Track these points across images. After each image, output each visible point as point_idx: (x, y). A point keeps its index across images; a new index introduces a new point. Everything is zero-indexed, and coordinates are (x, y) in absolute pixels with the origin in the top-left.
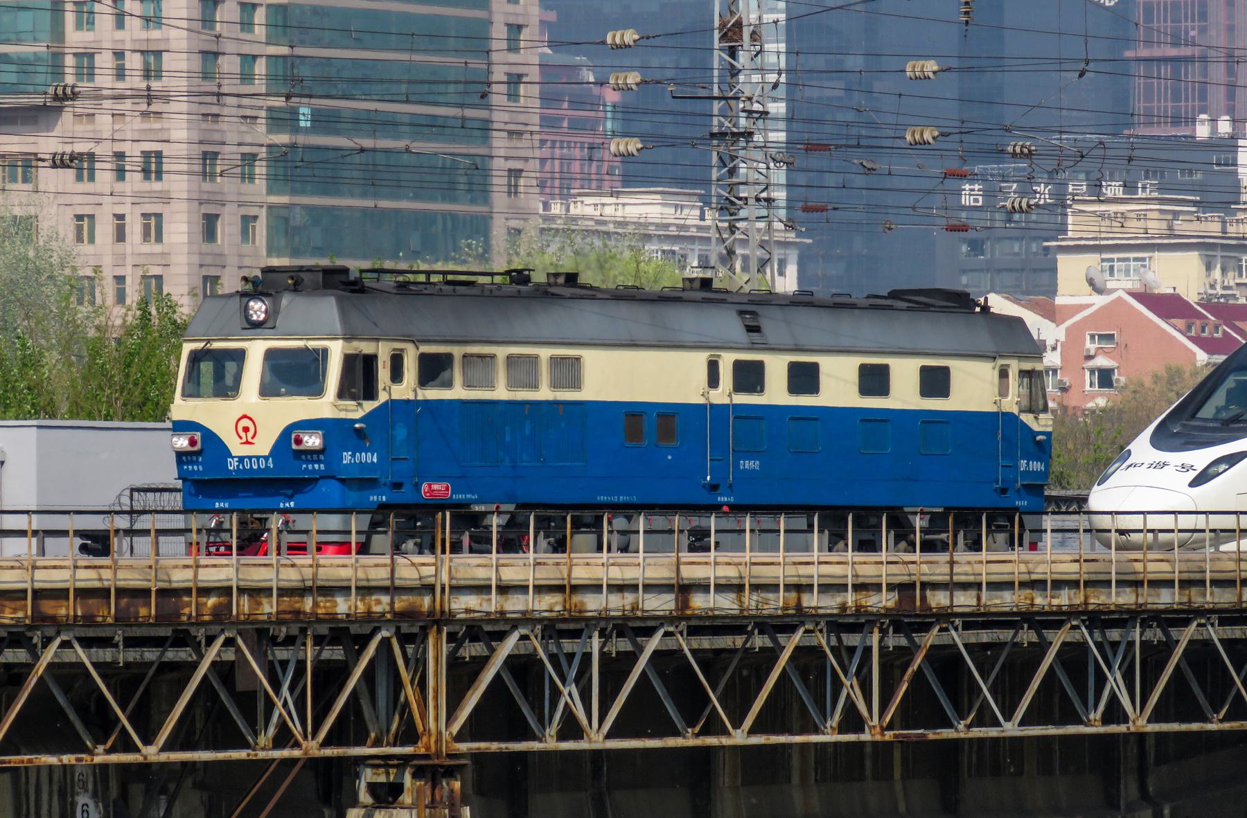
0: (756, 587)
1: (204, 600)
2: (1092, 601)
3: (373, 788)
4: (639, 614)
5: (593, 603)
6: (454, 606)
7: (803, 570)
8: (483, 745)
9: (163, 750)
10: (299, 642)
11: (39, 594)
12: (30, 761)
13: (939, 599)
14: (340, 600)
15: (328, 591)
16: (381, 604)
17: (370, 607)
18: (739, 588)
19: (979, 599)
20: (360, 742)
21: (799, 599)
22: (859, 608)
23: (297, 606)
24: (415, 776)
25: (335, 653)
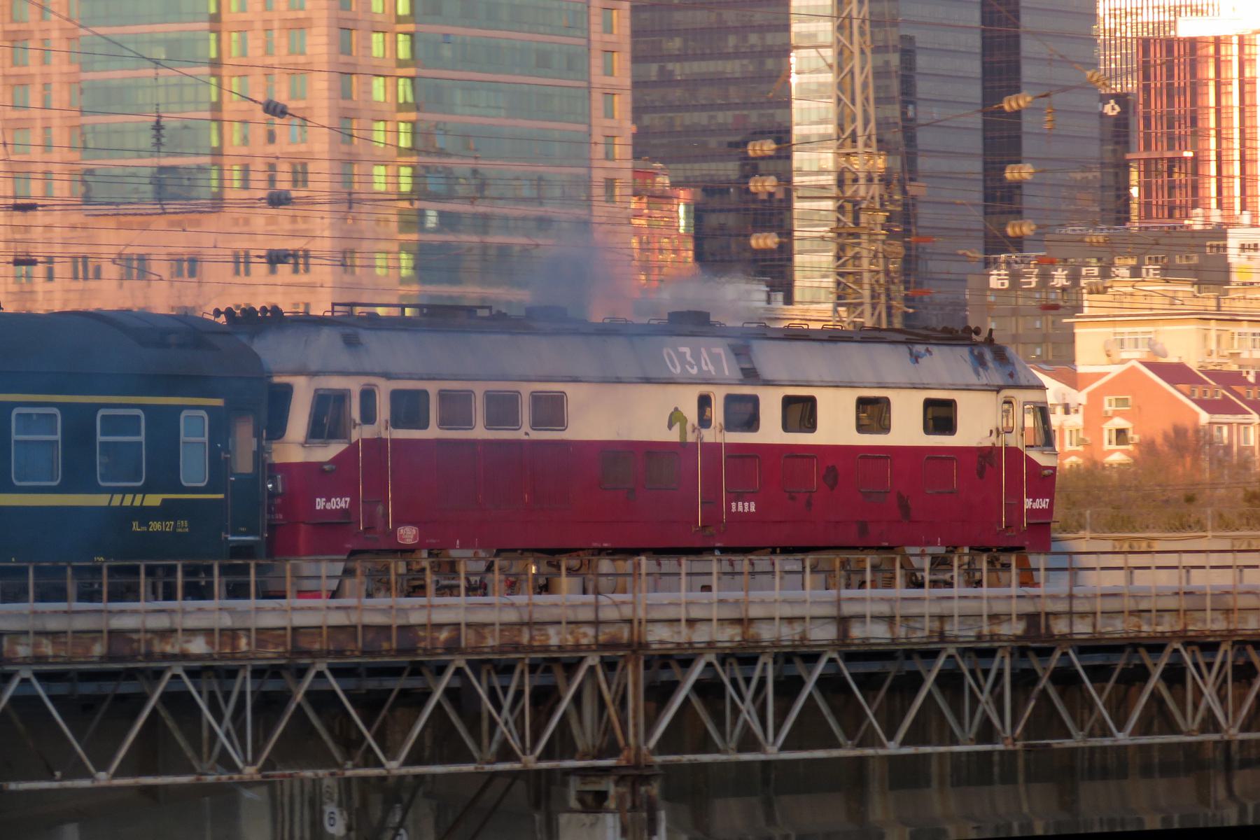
0: (906, 618)
1: (436, 634)
2: (1190, 628)
4: (807, 643)
5: (766, 633)
6: (650, 638)
7: (945, 604)
13: (1060, 627)
14: (552, 631)
18: (890, 620)
19: (1094, 626)
20: (572, 758)
24: (617, 783)
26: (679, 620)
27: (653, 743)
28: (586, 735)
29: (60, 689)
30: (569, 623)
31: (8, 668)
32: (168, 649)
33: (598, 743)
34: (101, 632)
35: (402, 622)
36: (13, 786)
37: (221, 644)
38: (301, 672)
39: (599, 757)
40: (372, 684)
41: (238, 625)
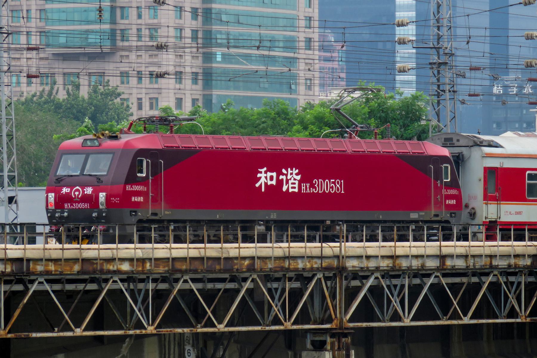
0: (474, 256)
1: (243, 262)
3: (313, 343)
5: (405, 264)
8: (359, 324)
9: (226, 326)
10: (282, 280)
11: (174, 259)
12: (171, 331)
14: (300, 261)
15: (295, 258)
16: (316, 264)
18: (466, 257)
21: (491, 261)
22: (516, 265)
23: (282, 264)
24: (331, 337)
25: (297, 285)
26: (362, 256)
27: (348, 317)
28: (316, 311)
29: (57, 287)
30: (308, 257)
31: (32, 278)
32: (111, 268)
33: (321, 317)
35: (225, 255)
36: (34, 335)
37: (137, 266)
38: (177, 281)
39: (322, 324)
40: (210, 286)
41: (145, 256)
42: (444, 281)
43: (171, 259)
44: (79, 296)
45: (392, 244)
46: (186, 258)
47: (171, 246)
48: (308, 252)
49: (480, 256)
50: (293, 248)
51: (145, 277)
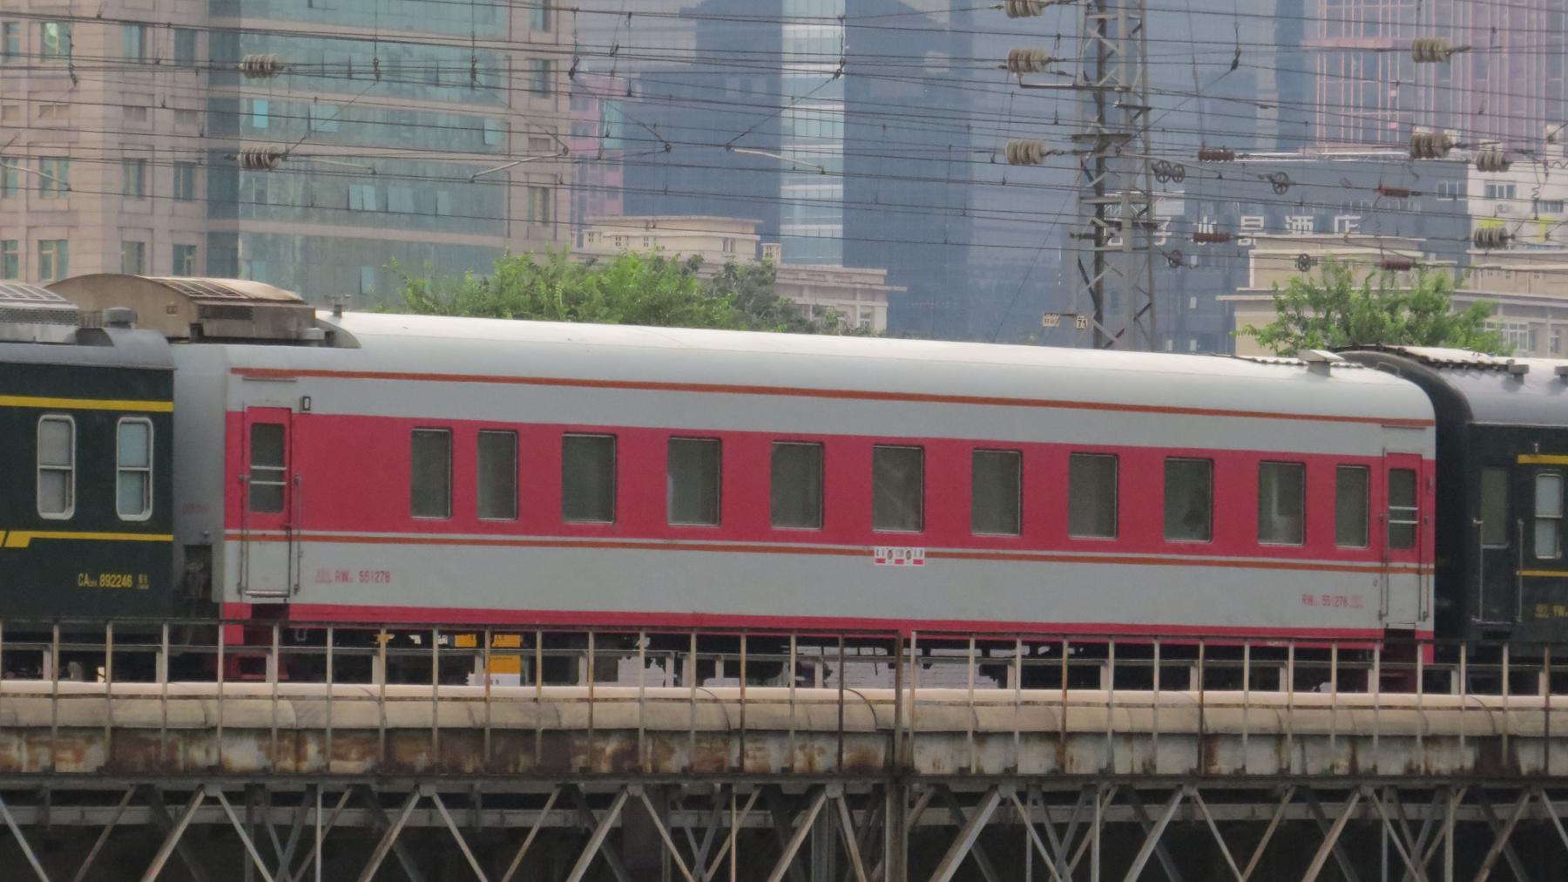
0: (1302, 738)
1: (599, 745)
11: (392, 732)
13: (1528, 759)
15: (759, 734)
17: (810, 763)
18: (1279, 737)
23: (720, 754)
26: (964, 733)
30: (798, 732)
32: (198, 755)
34: (102, 729)
35: (546, 724)
37: (279, 752)
38: (398, 800)
40: (490, 818)
41: (304, 724)
42: (1209, 814)
43: (382, 733)
44: (99, 844)
45: (1054, 694)
46: (427, 731)
47: (383, 690)
48: (800, 717)
49: (1321, 737)
50: (754, 702)
51: (304, 789)
